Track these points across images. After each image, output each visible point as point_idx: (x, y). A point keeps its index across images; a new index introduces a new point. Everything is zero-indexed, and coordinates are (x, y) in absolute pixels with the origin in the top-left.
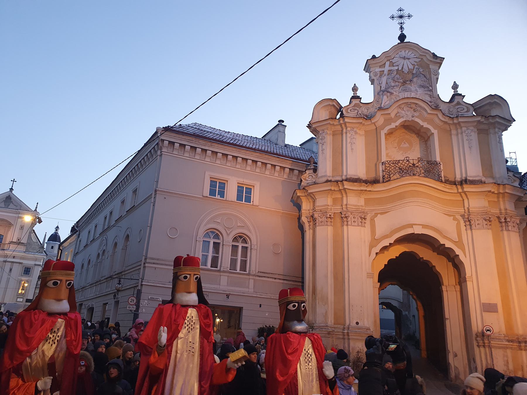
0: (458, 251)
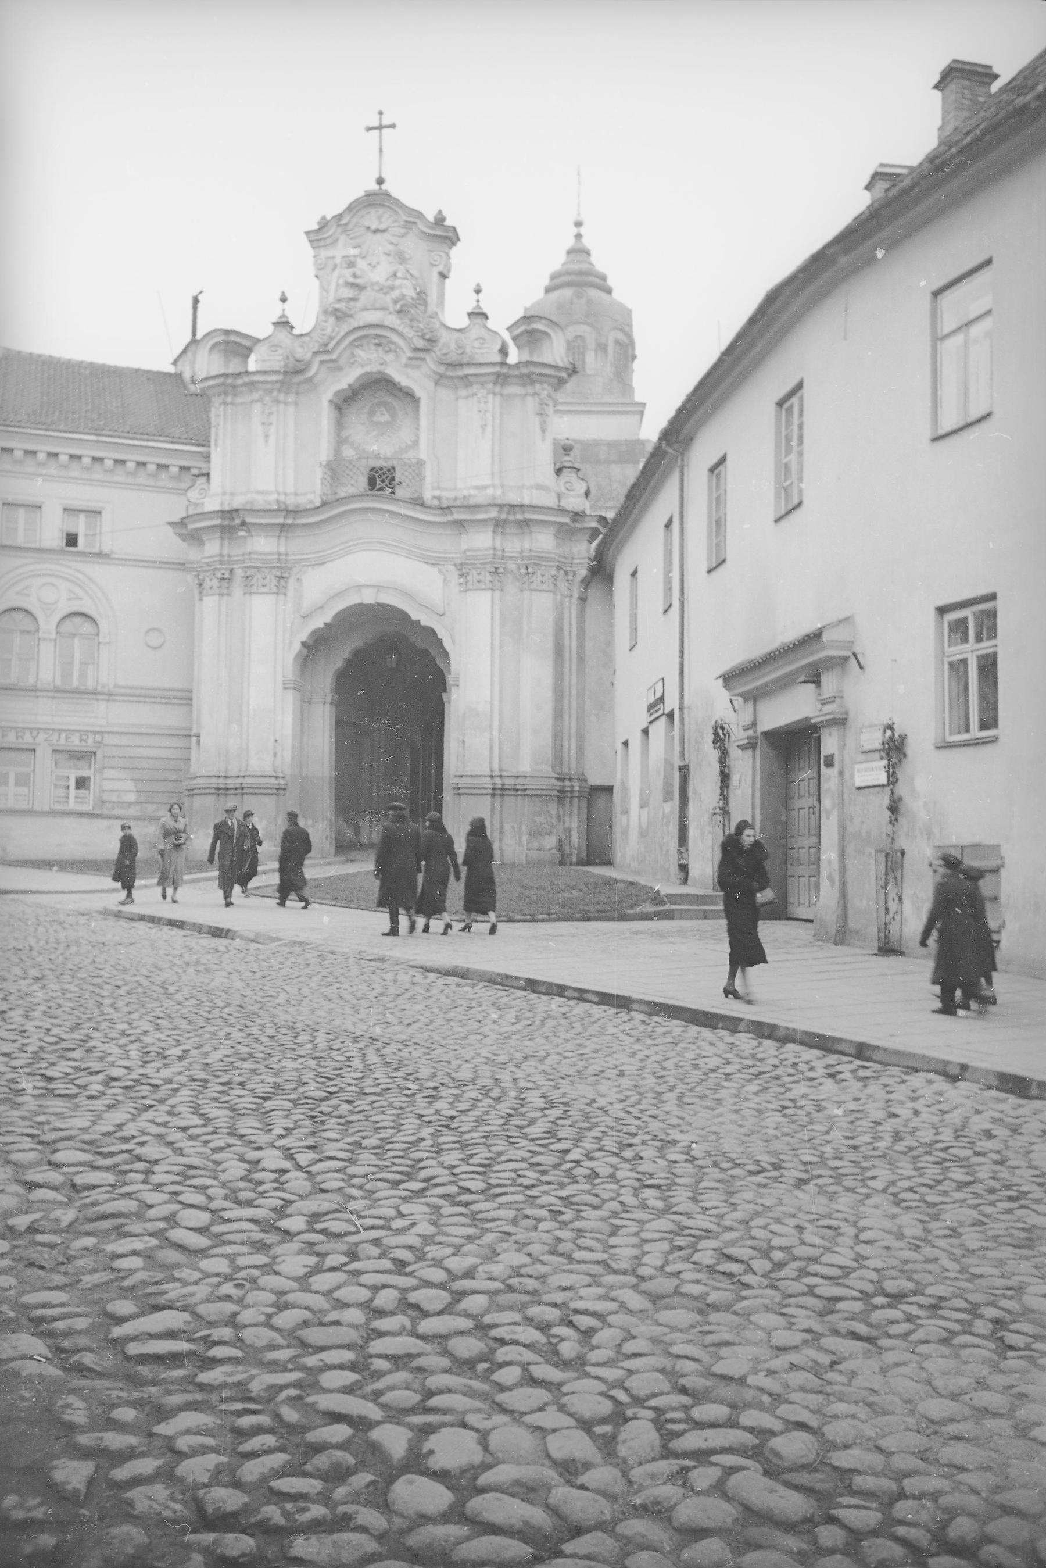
0: (441, 634)
